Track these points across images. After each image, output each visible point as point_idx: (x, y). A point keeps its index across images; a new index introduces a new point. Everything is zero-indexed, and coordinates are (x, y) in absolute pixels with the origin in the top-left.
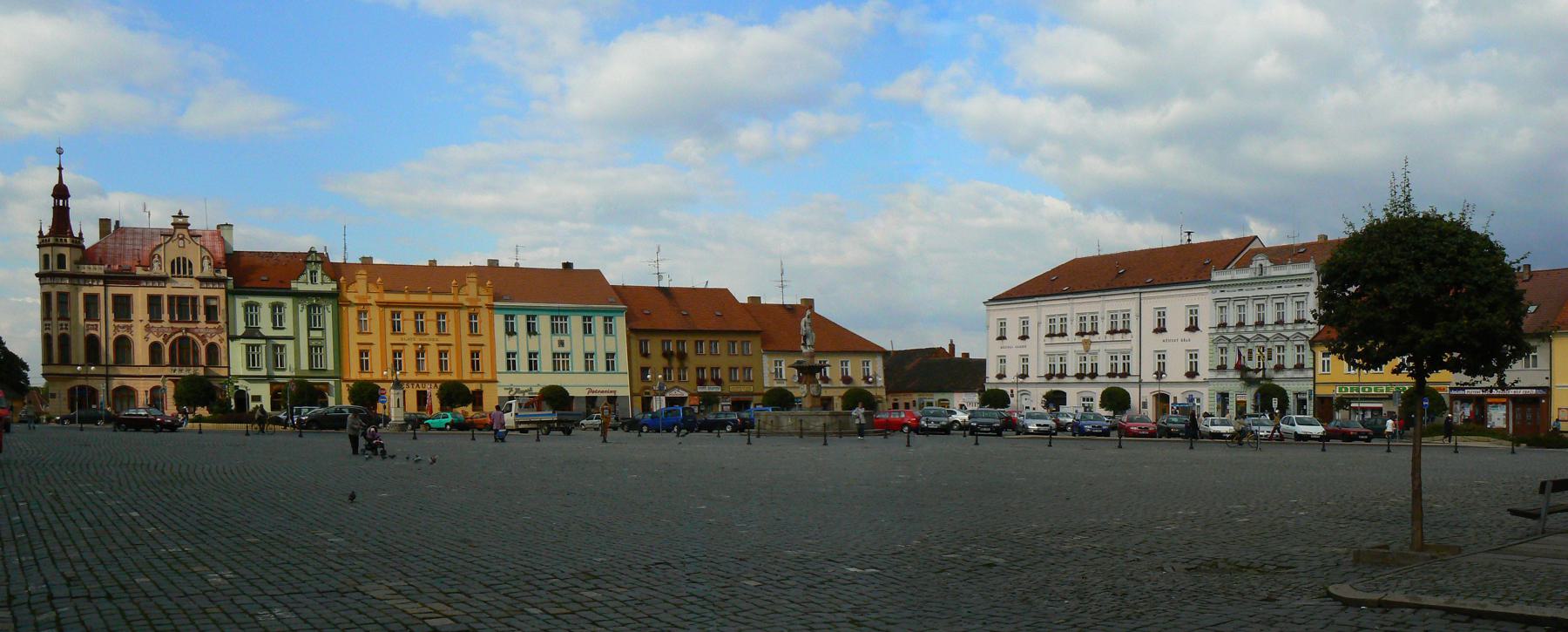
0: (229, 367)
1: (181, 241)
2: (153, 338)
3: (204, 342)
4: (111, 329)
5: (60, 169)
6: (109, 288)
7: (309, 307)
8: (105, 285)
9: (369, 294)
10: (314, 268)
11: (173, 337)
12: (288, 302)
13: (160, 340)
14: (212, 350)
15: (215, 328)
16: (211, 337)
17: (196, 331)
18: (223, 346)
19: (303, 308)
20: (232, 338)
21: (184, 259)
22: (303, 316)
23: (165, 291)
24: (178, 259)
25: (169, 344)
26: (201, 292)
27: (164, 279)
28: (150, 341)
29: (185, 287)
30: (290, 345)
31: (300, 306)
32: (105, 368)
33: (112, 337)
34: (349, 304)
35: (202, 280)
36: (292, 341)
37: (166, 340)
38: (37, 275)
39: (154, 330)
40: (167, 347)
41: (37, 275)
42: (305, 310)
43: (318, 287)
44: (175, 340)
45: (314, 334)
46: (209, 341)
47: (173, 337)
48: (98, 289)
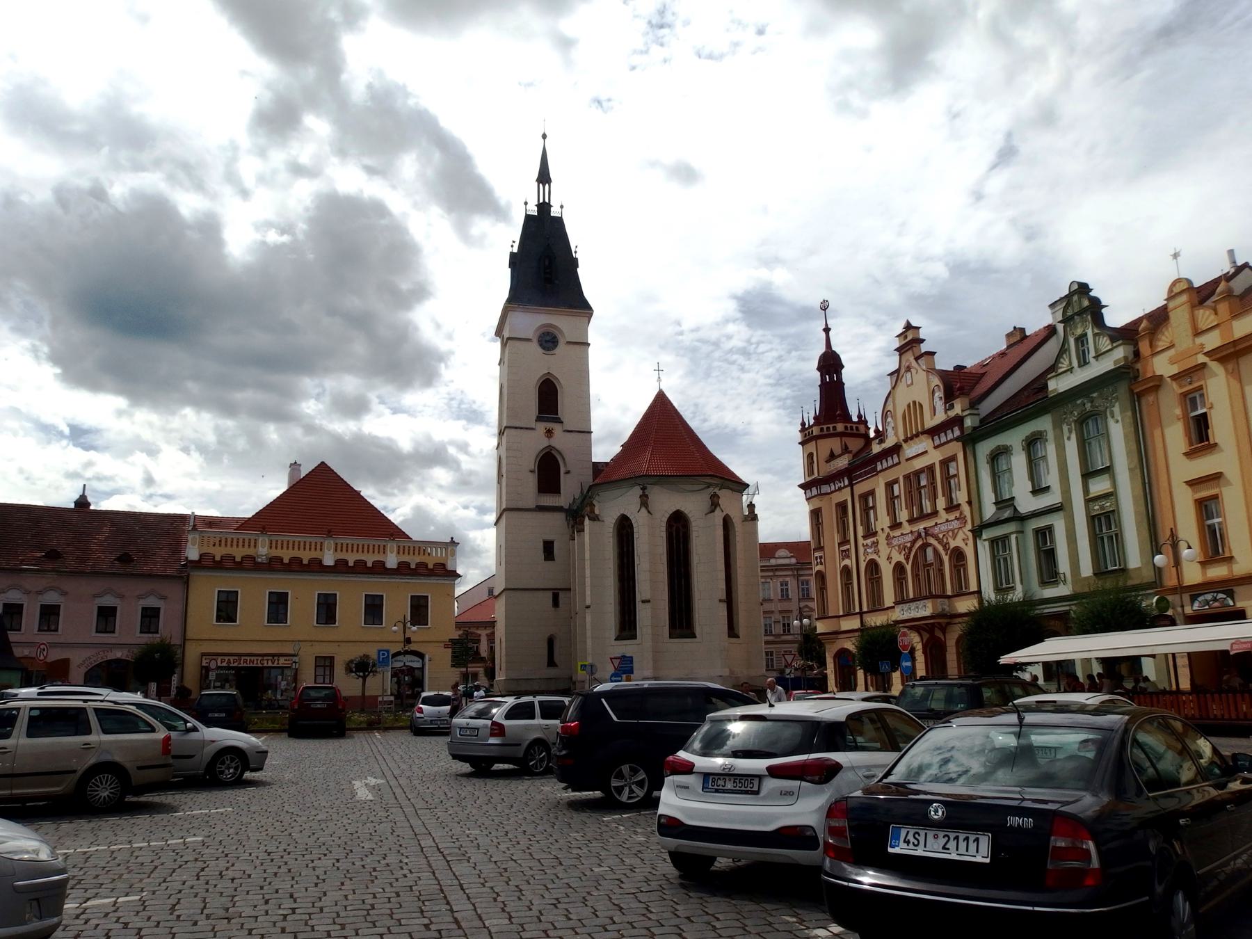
0: (979, 592)
1: (909, 375)
2: (898, 557)
3: (945, 547)
4: (861, 550)
5: (827, 330)
6: (855, 487)
7: (1082, 422)
8: (851, 485)
9: (1199, 340)
10: (1079, 331)
11: (914, 550)
12: (1044, 424)
13: (902, 559)
14: (958, 555)
15: (956, 519)
16: (954, 538)
17: (936, 530)
18: (969, 552)
19: (1070, 431)
20: (977, 532)
21: (914, 402)
22: (1072, 447)
23: (899, 473)
24: (909, 406)
25: (910, 562)
26: (935, 457)
27: (896, 449)
28: (893, 563)
29: (922, 453)
30: (1058, 524)
31: (1065, 428)
32: (859, 616)
33: (863, 566)
34: (1157, 383)
35: (934, 432)
36: (1061, 514)
37: (907, 559)
38: (801, 486)
39: (895, 542)
40: (909, 568)
41: (801, 486)
42: (1074, 436)
43: (1098, 368)
44: (916, 553)
45: (1099, 486)
46: (953, 544)
47: (914, 550)
48: (845, 495)
